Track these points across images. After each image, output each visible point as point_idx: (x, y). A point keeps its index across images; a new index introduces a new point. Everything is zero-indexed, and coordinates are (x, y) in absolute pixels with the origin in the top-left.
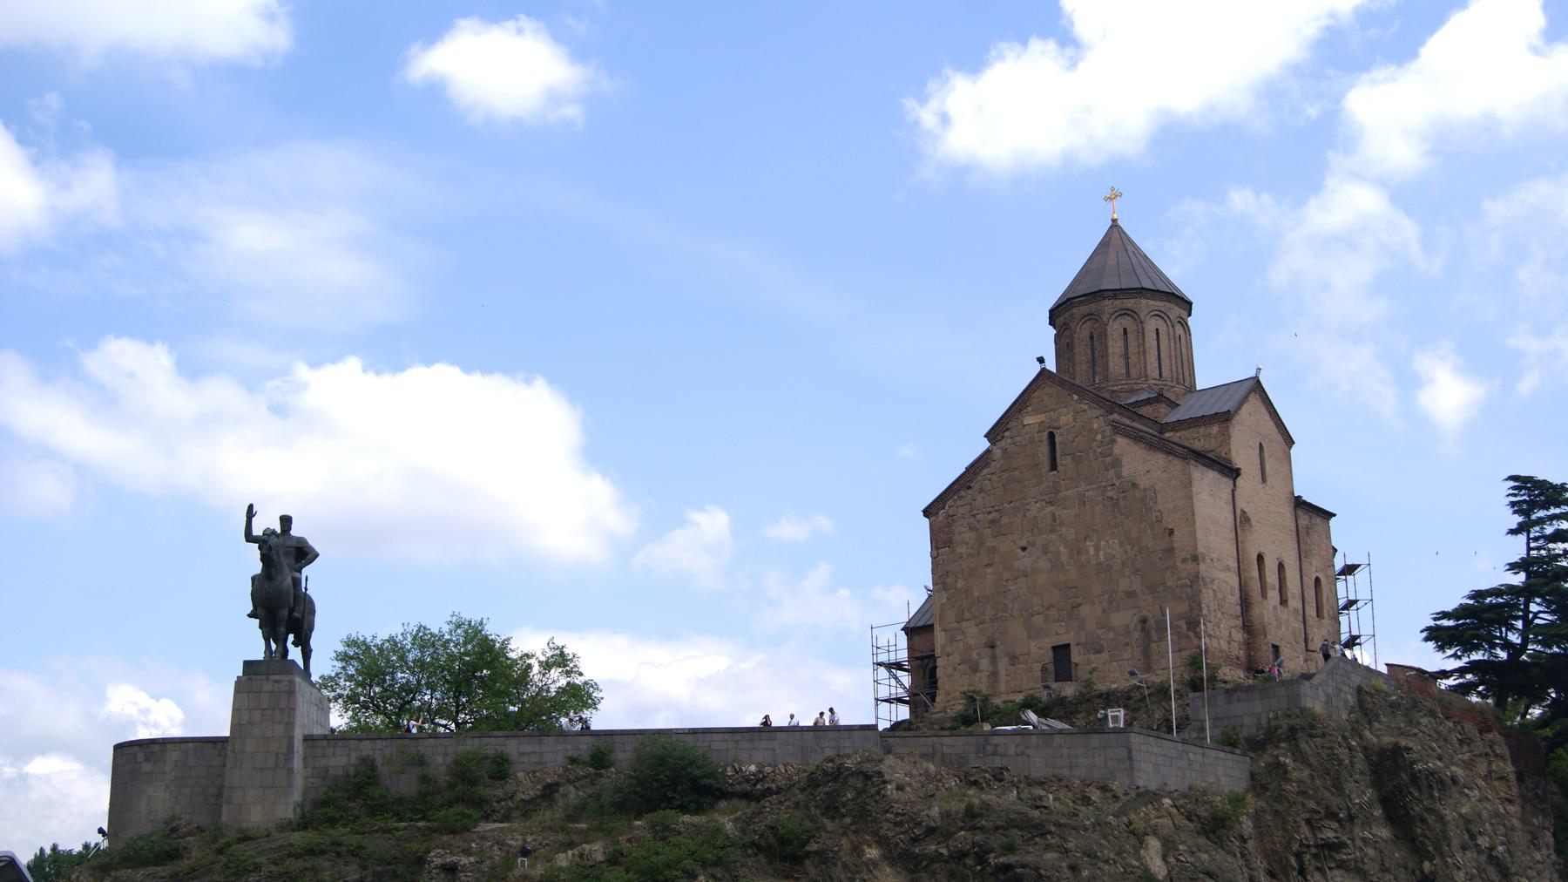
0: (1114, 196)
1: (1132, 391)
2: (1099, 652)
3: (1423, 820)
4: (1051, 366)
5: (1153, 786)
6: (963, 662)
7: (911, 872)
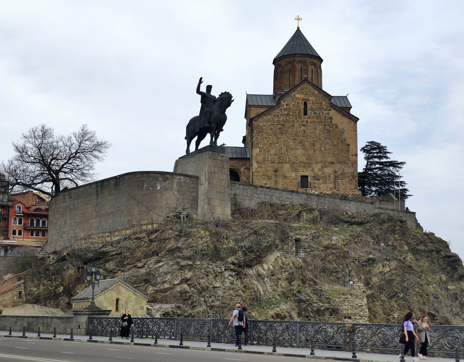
6: (264, 175)
7: (414, 255)
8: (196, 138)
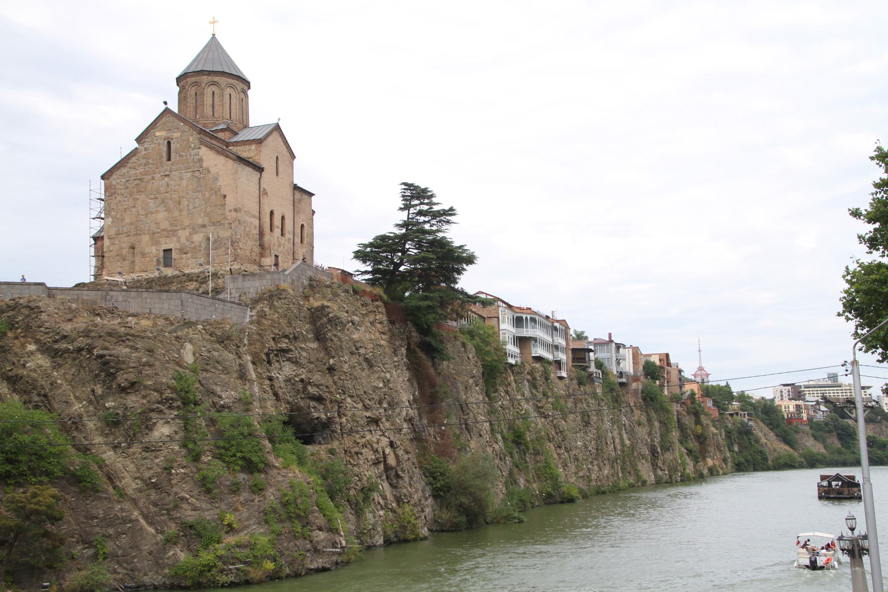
0: (214, 22)
1: (216, 125)
2: (186, 253)
3: (332, 340)
4: (174, 107)
5: (194, 319)
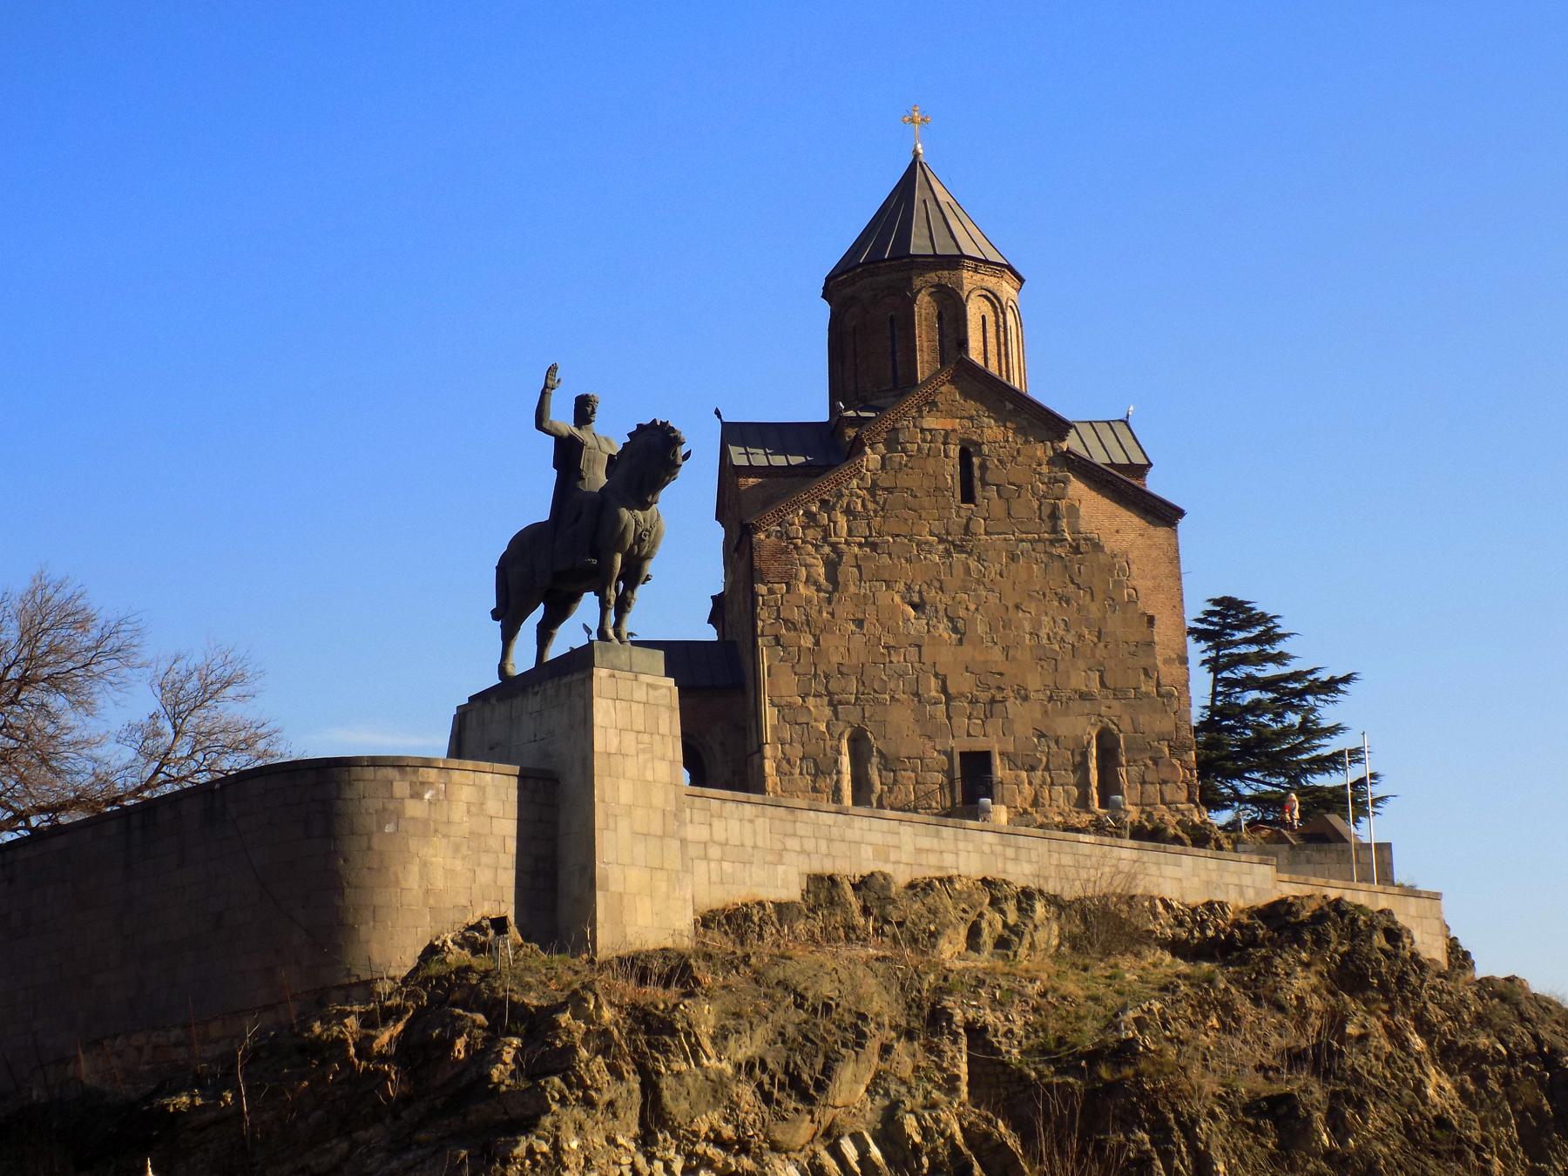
2: (1033, 769)
8: (538, 613)
